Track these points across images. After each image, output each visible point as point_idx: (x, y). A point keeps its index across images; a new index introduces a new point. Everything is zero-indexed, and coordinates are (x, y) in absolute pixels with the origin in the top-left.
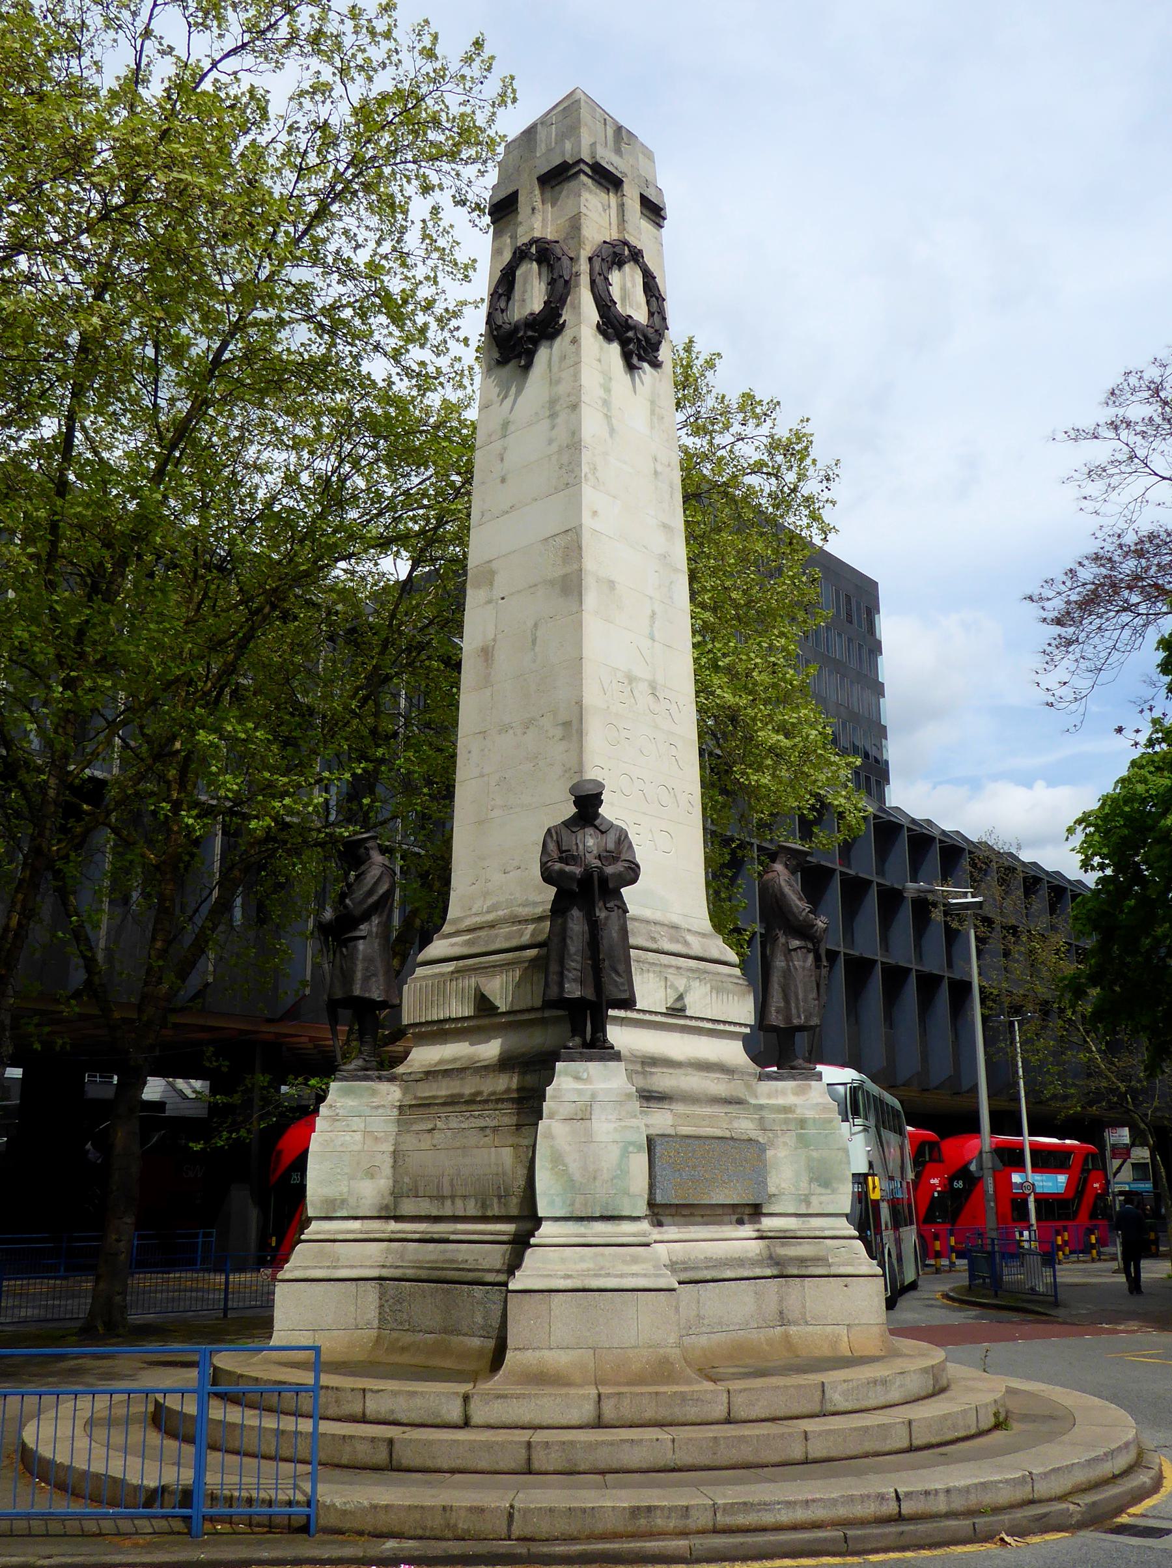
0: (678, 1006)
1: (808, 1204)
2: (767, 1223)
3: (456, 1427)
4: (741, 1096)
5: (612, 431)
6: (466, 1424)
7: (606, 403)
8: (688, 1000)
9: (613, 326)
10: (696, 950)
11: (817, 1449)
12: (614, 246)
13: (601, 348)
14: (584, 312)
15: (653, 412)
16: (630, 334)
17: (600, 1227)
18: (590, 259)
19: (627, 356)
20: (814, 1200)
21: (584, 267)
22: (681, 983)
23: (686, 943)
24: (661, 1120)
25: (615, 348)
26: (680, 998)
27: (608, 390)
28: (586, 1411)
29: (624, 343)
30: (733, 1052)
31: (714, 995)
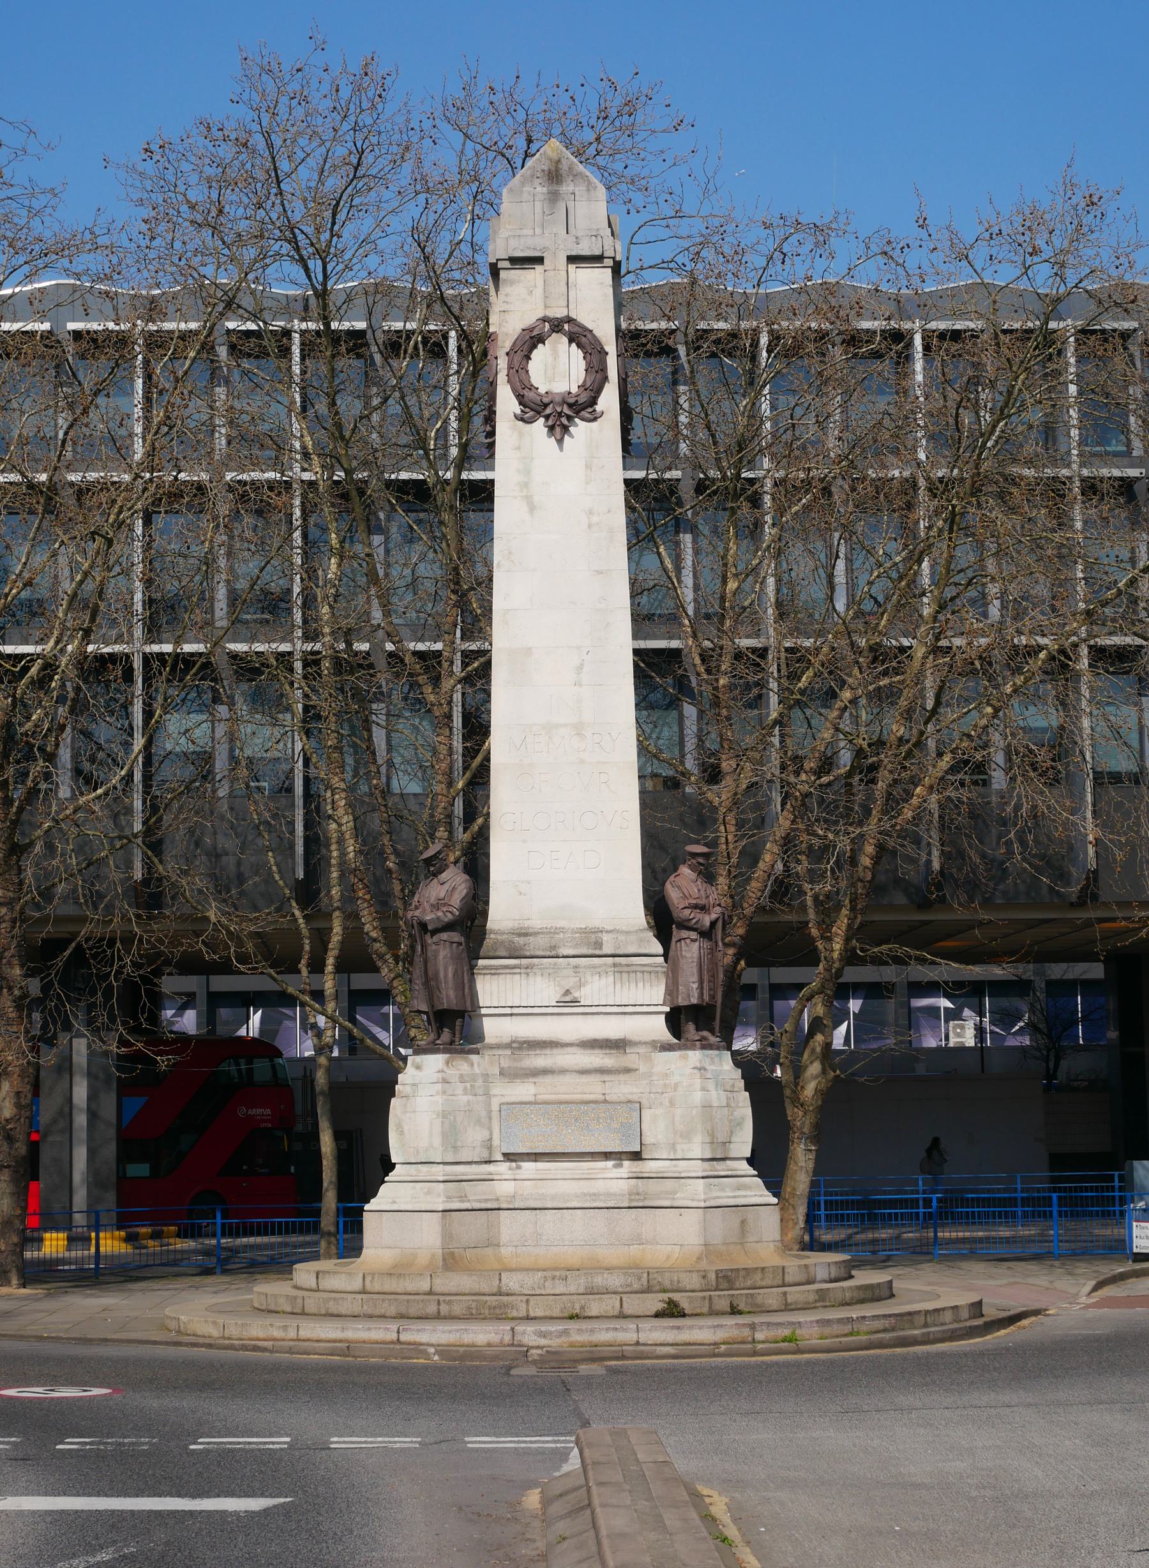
0: (568, 999)
1: (675, 1151)
2: (649, 1167)
3: (311, 1290)
4: (635, 1066)
5: (532, 508)
6: (318, 1290)
7: (525, 485)
9: (533, 407)
10: (607, 950)
12: (531, 329)
13: (521, 435)
14: (506, 403)
15: (588, 467)
16: (548, 411)
17: (424, 1168)
18: (507, 354)
19: (551, 429)
20: (678, 1147)
21: (503, 363)
22: (570, 983)
23: (599, 944)
24: (524, 1090)
26: (567, 992)
27: (527, 472)
29: (547, 417)
30: (657, 1027)
31: (618, 986)
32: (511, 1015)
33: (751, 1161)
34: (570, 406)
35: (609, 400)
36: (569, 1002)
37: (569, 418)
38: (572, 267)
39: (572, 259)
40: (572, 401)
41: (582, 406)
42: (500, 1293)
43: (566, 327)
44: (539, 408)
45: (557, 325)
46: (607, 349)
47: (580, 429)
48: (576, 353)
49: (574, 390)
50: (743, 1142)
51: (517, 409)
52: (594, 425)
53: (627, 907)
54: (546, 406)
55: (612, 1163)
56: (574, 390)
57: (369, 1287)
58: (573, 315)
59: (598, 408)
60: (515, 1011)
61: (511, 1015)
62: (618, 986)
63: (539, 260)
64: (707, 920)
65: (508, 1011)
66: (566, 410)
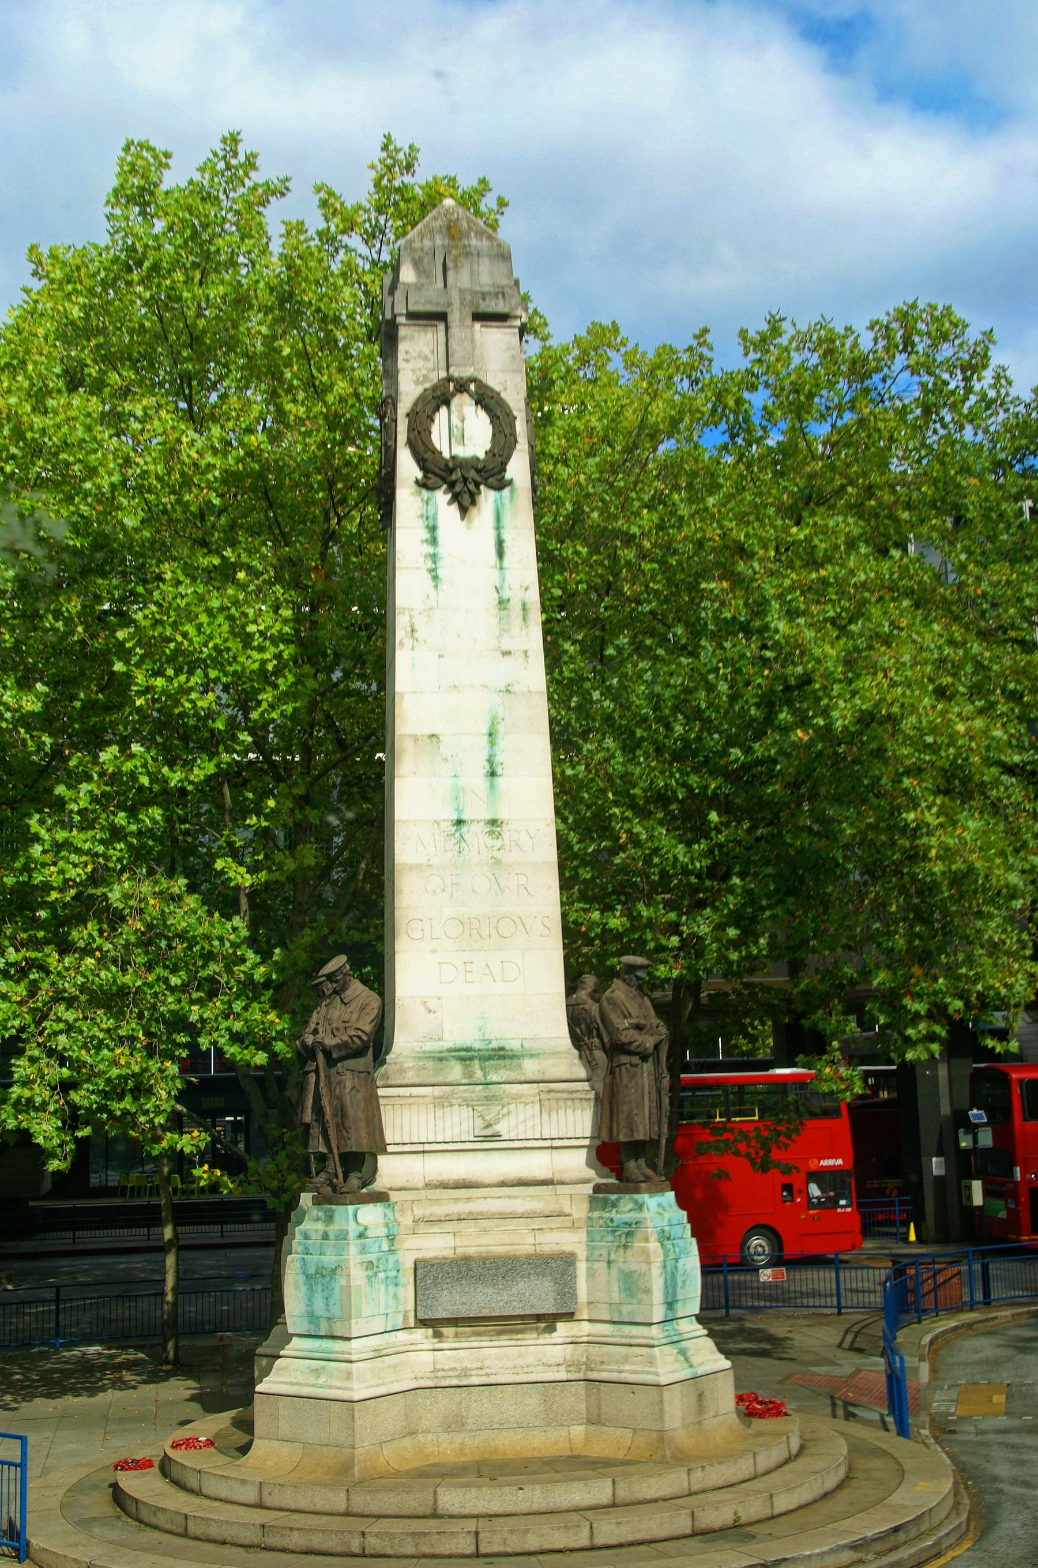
0: (489, 1132)
8: (501, 1128)
9: (437, 472)
11: (374, 1544)
19: (456, 498)
25: (441, 497)
27: (433, 541)
28: (250, 1495)
29: (451, 486)
31: (545, 1116)
32: (424, 1152)
33: (700, 1319)
34: (479, 471)
35: (518, 468)
36: (489, 1139)
37: (477, 485)
38: (477, 326)
39: (479, 317)
40: (480, 466)
41: (490, 472)
42: (435, 1515)
43: (472, 387)
44: (443, 474)
45: (462, 387)
46: (515, 413)
47: (488, 498)
48: (484, 418)
49: (482, 456)
50: (692, 1299)
51: (420, 475)
52: (506, 491)
53: (552, 1027)
54: (451, 471)
55: (543, 1325)
56: (482, 456)
57: (268, 1501)
58: (481, 376)
59: (508, 476)
60: (427, 1147)
61: (424, 1152)
62: (545, 1116)
63: (441, 317)
64: (649, 1042)
65: (420, 1148)
66: (472, 474)
